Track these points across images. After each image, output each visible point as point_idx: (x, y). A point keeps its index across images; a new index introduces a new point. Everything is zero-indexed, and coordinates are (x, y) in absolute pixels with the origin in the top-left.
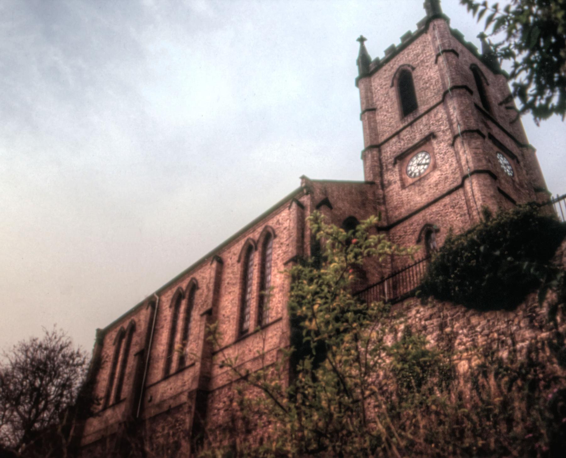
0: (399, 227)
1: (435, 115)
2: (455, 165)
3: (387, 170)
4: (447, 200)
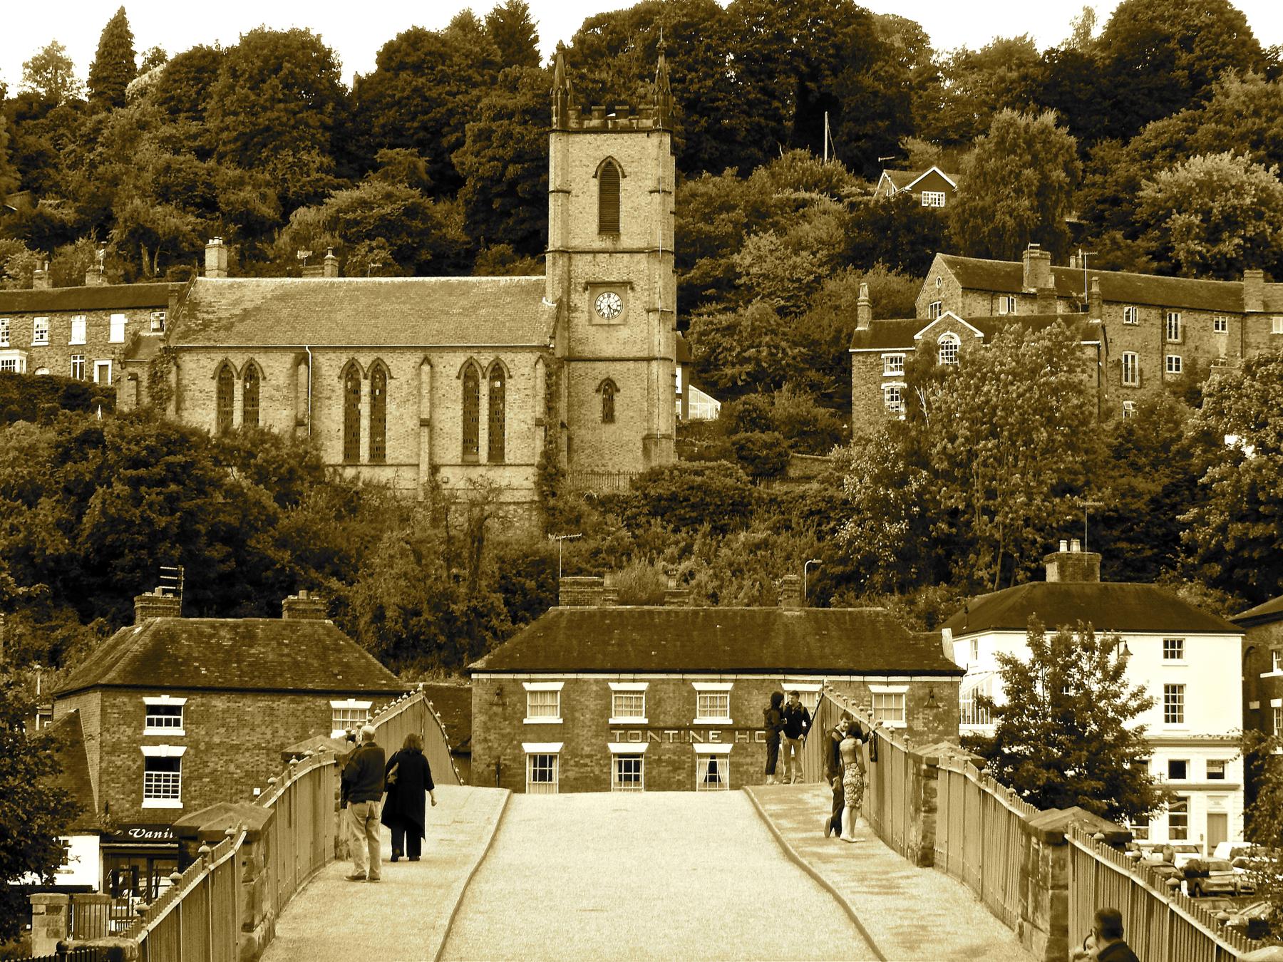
0: (580, 365)
1: (638, 263)
2: (645, 334)
3: (576, 291)
4: (631, 365)
